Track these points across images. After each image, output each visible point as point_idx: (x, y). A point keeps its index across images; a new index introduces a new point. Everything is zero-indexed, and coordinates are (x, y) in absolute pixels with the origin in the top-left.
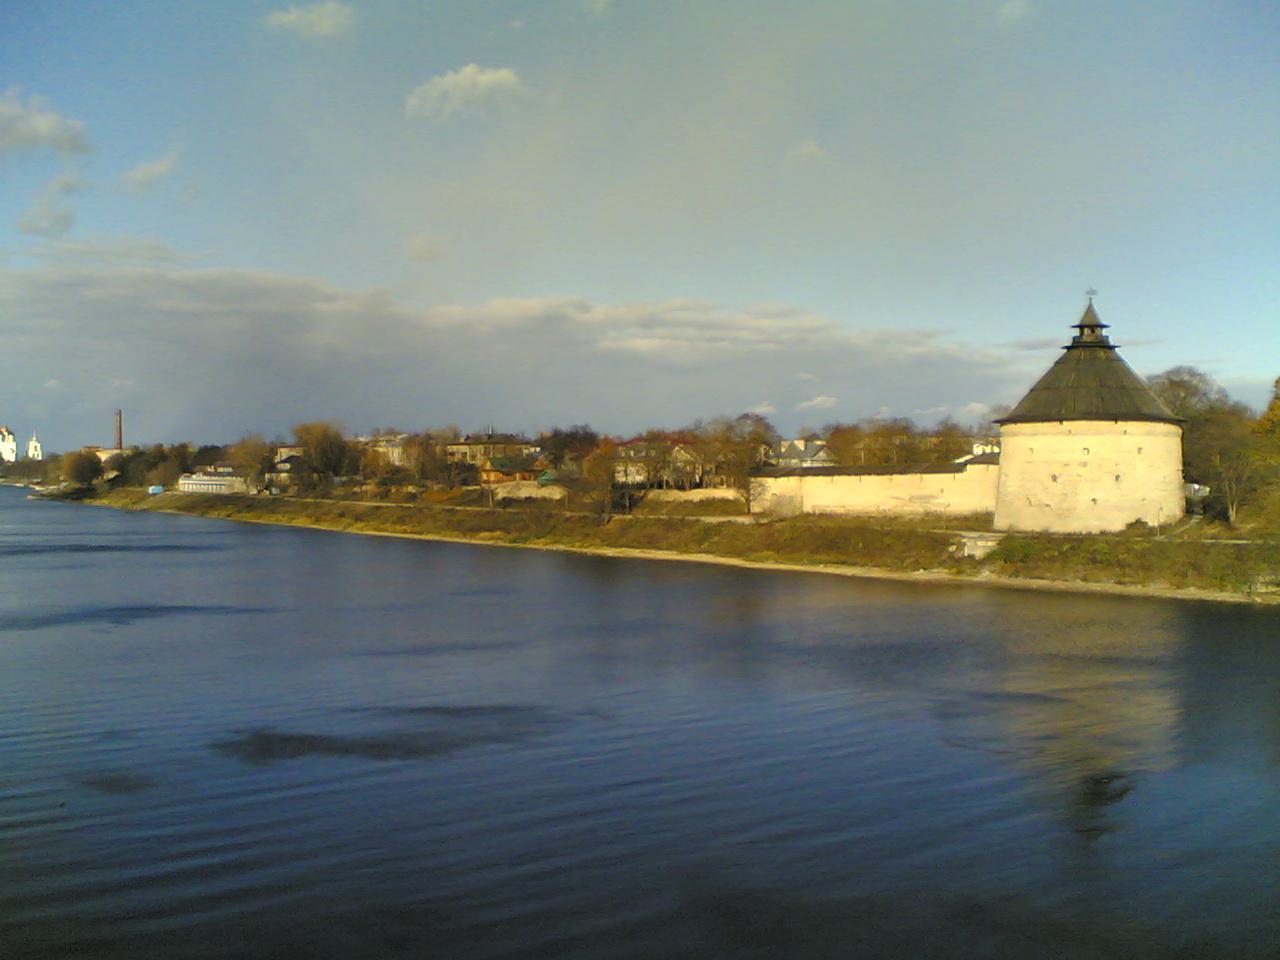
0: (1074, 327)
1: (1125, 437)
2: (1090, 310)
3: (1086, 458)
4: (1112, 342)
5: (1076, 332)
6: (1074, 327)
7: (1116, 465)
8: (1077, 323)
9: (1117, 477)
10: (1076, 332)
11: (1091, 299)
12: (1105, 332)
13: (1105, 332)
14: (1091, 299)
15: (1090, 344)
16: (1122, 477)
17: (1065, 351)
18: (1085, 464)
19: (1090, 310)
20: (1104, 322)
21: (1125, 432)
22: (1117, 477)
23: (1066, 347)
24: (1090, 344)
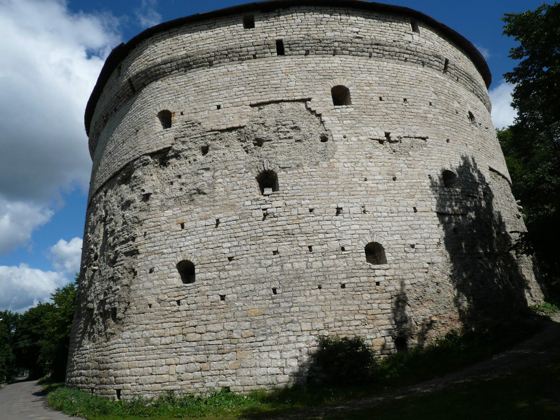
1: (285, 62)
16: (282, 178)
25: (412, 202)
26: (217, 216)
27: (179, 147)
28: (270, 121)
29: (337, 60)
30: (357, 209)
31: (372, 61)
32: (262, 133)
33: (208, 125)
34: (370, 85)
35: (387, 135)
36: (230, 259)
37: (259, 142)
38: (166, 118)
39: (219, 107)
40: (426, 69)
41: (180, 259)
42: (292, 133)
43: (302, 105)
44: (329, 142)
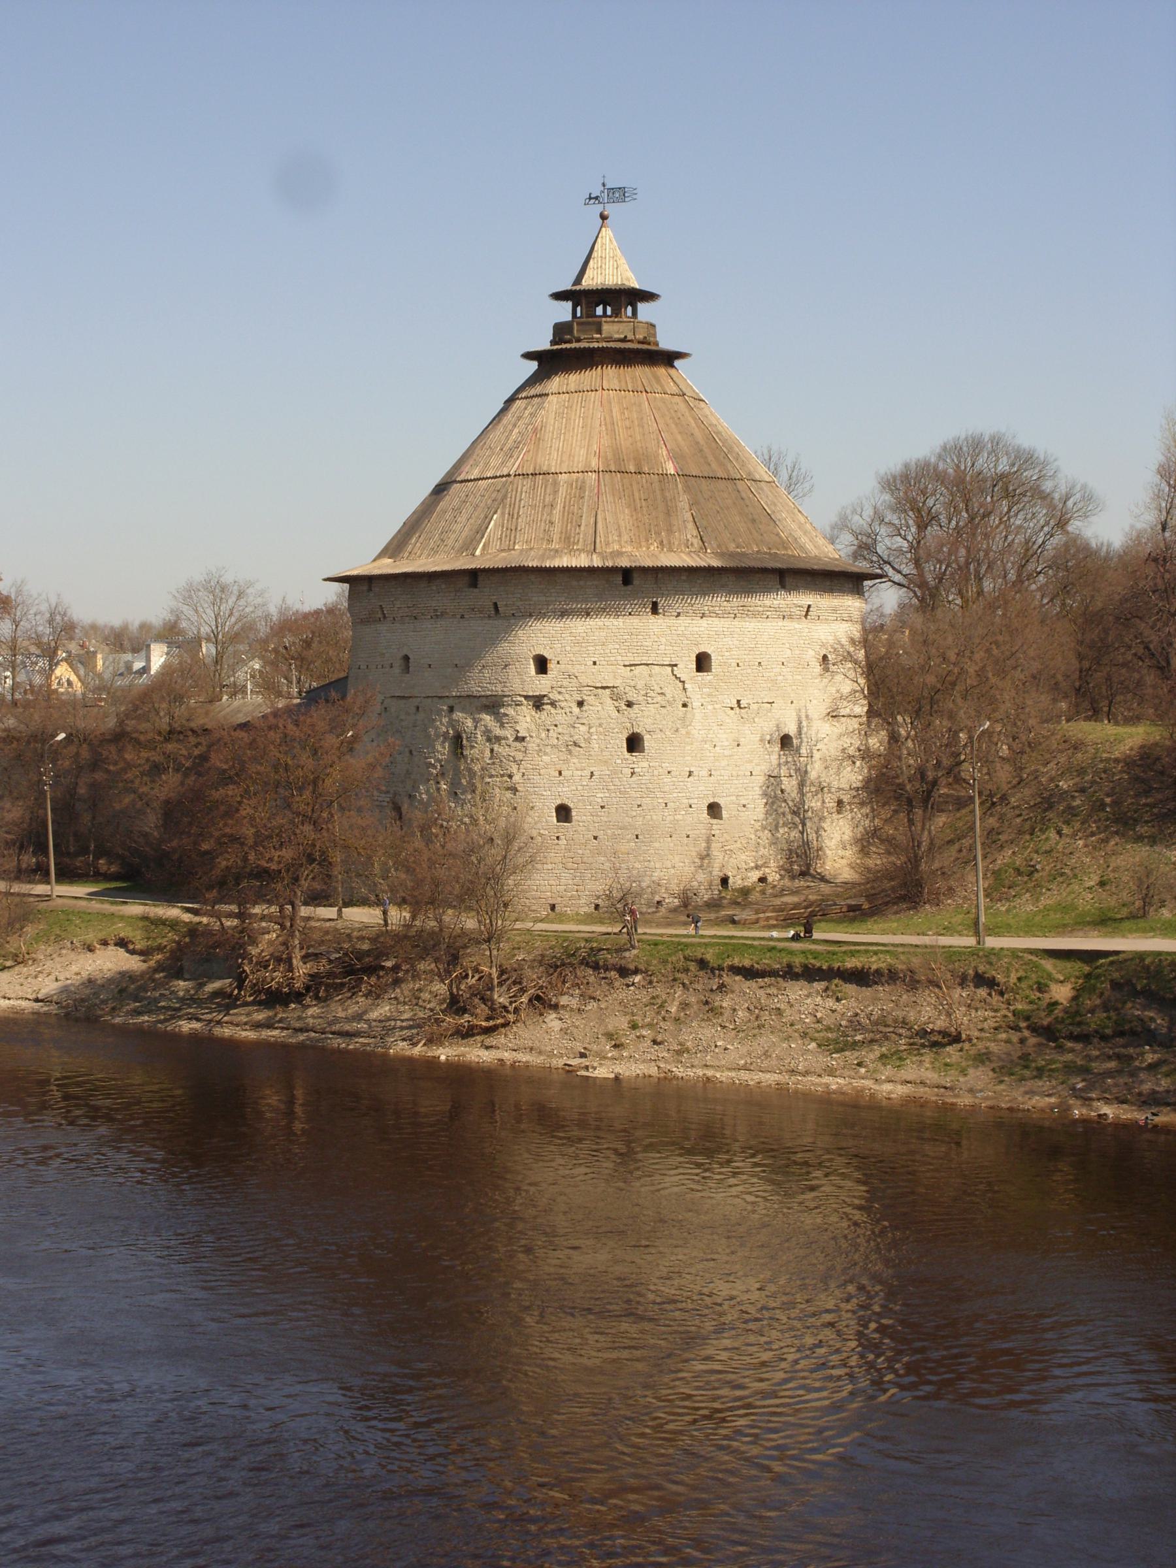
0: (559, 296)
3: (540, 685)
4: (665, 342)
5: (564, 312)
6: (559, 296)
8: (566, 285)
9: (634, 743)
16: (648, 743)
17: (533, 366)
22: (634, 743)
23: (529, 356)
25: (750, 768)
26: (592, 769)
27: (554, 696)
28: (640, 684)
29: (704, 622)
30: (705, 773)
31: (736, 622)
32: (632, 696)
33: (584, 680)
34: (729, 650)
35: (738, 701)
36: (602, 807)
37: (629, 704)
38: (542, 665)
39: (595, 663)
40: (786, 623)
41: (559, 802)
42: (659, 698)
44: (689, 709)
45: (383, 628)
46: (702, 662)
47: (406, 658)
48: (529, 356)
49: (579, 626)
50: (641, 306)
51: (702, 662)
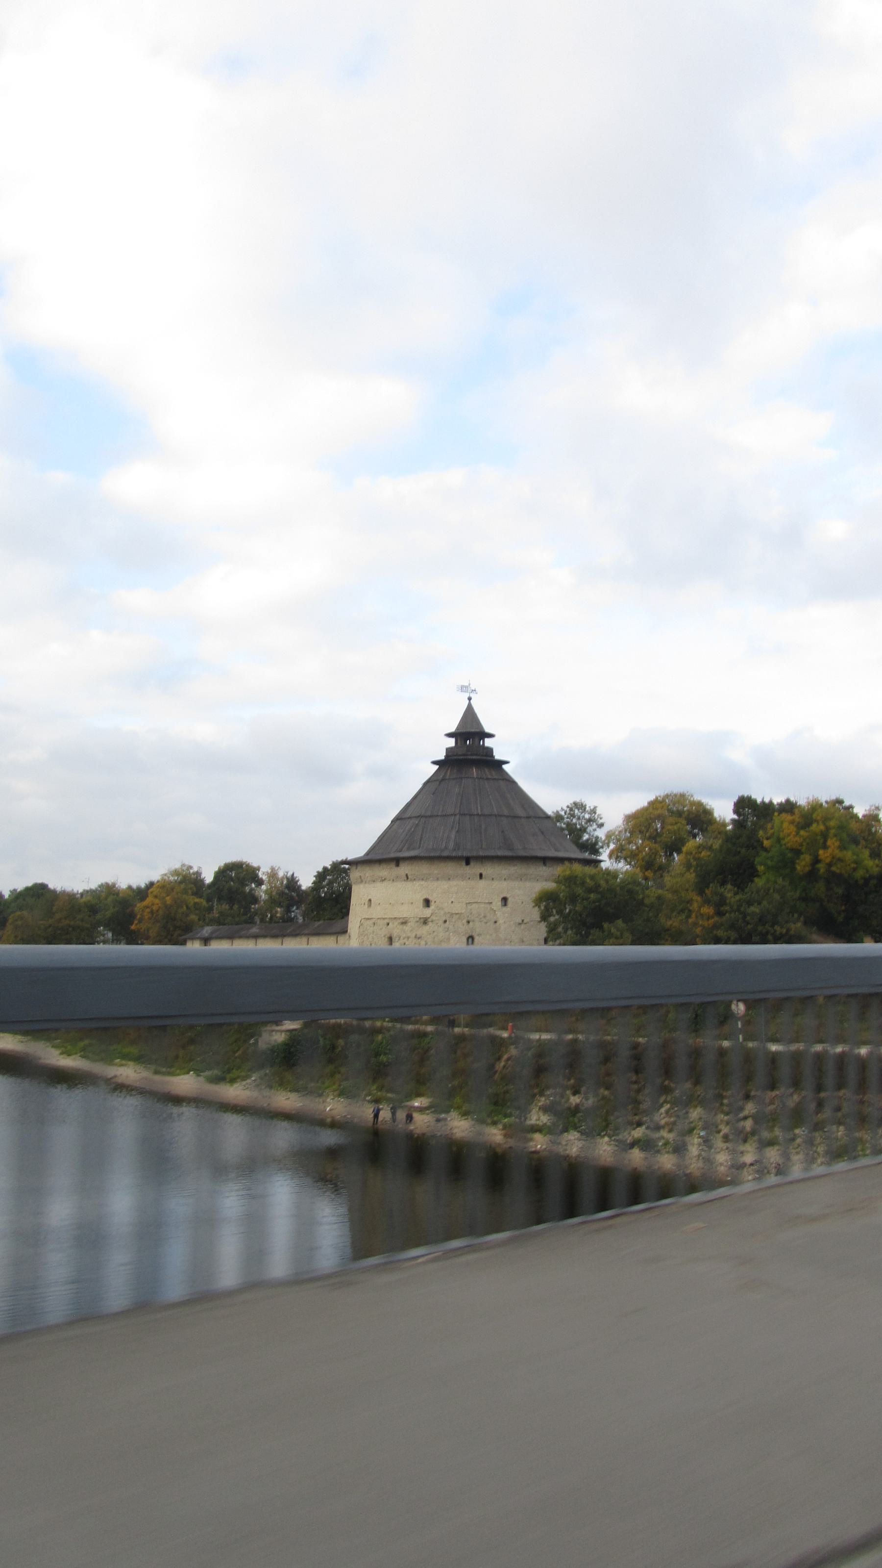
0: (450, 735)
1: (482, 883)
2: (470, 714)
3: (427, 912)
4: (498, 756)
5: (451, 742)
6: (450, 735)
7: (468, 922)
10: (451, 742)
11: (470, 699)
12: (488, 742)
13: (488, 742)
14: (470, 699)
15: (470, 755)
16: (477, 939)
17: (437, 767)
18: (425, 921)
19: (470, 714)
20: (487, 730)
21: (481, 876)
23: (434, 763)
24: (470, 755)
27: (433, 918)
43: (488, 906)
45: (362, 886)
46: (505, 900)
47: (370, 900)
48: (434, 763)
49: (444, 885)
50: (486, 740)
51: (505, 900)
